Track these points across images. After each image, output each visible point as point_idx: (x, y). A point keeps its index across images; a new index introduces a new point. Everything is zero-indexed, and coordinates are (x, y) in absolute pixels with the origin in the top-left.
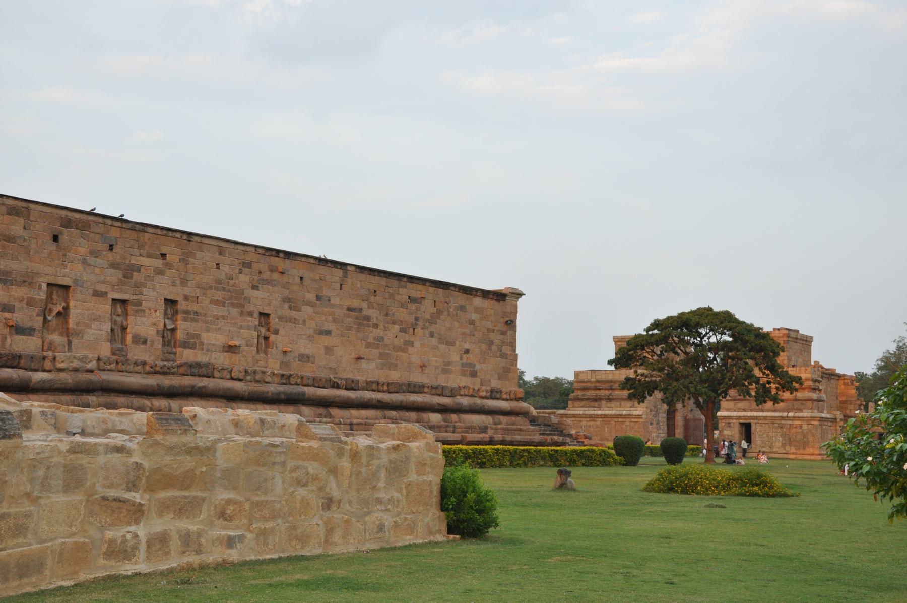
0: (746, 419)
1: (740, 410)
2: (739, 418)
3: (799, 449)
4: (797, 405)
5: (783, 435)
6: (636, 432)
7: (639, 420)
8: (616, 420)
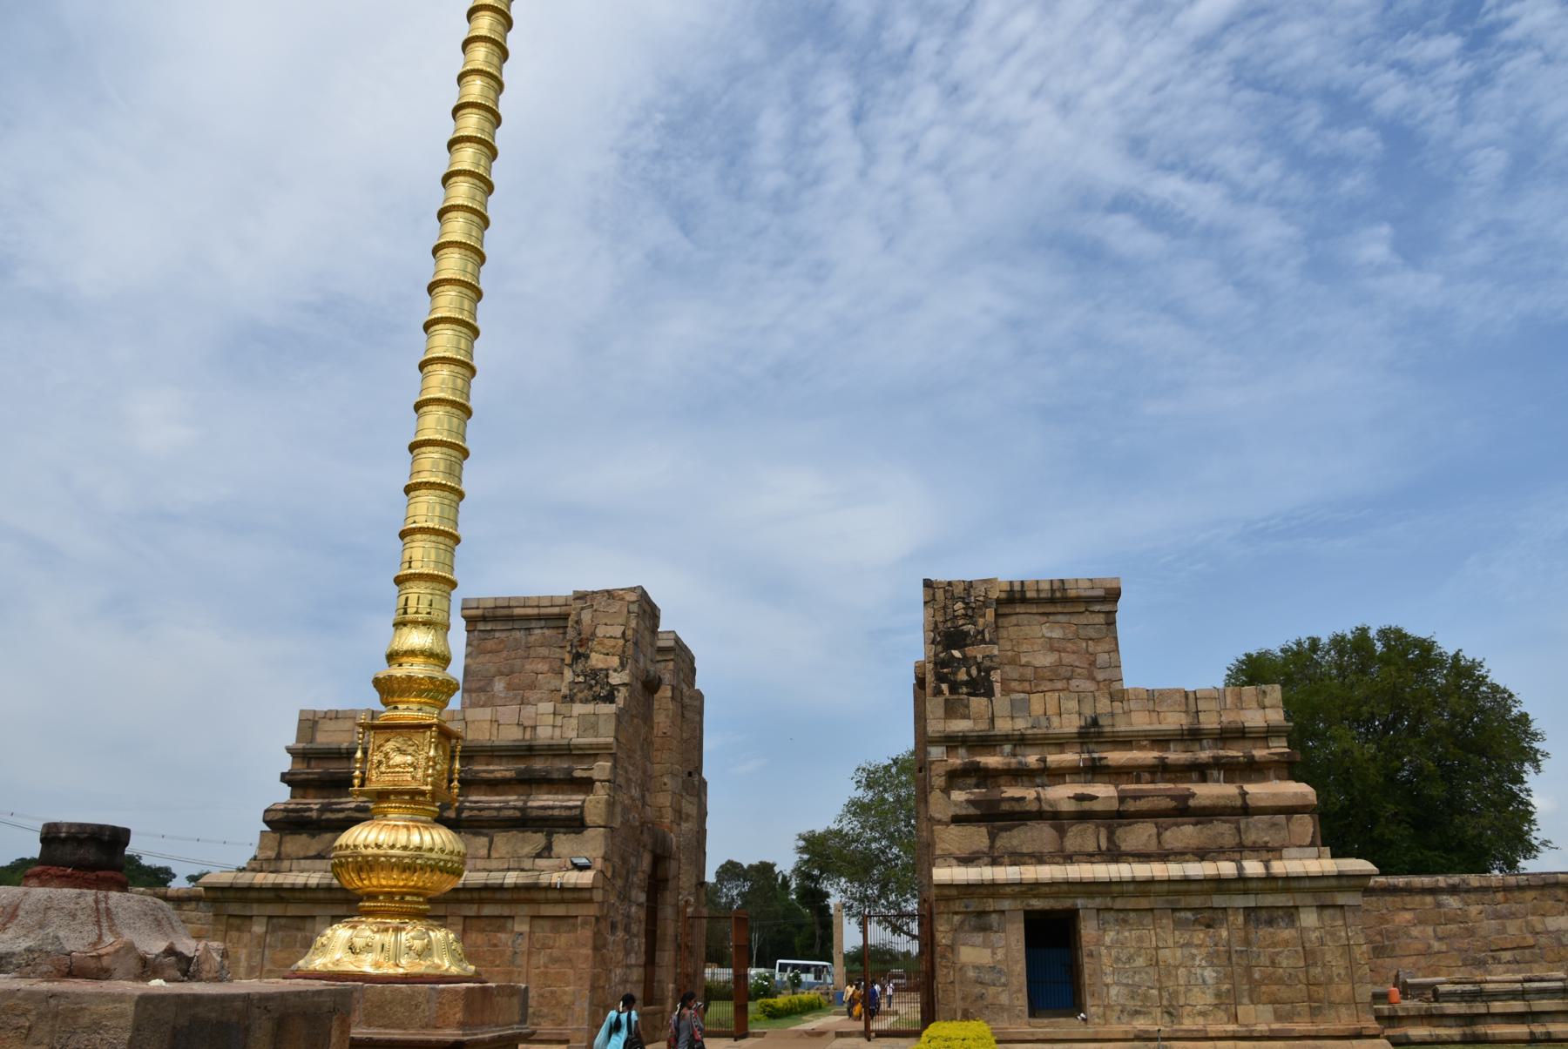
0: (1056, 896)
1: (1017, 858)
2: (1034, 887)
3: (1289, 1017)
4: (1257, 831)
5: (1223, 957)
6: (555, 960)
7: (574, 910)
8: (471, 910)
